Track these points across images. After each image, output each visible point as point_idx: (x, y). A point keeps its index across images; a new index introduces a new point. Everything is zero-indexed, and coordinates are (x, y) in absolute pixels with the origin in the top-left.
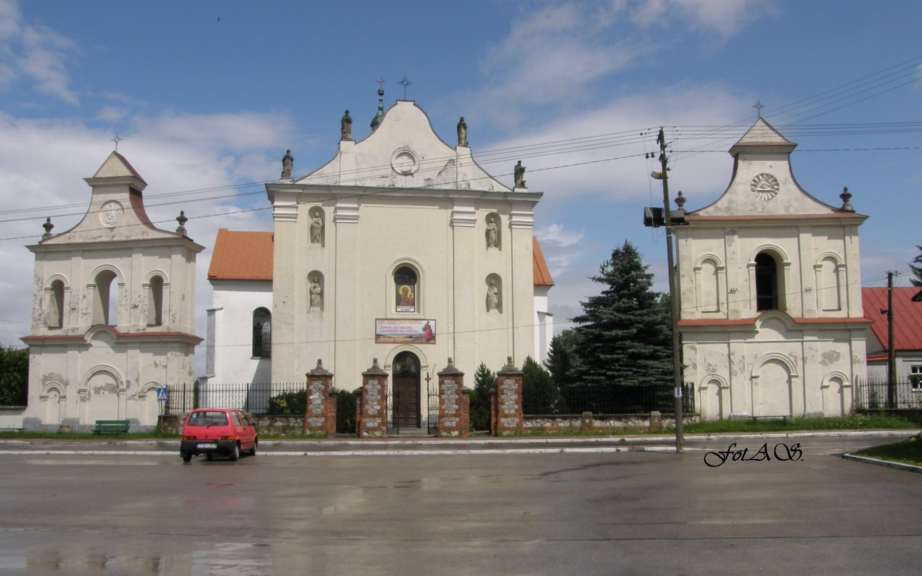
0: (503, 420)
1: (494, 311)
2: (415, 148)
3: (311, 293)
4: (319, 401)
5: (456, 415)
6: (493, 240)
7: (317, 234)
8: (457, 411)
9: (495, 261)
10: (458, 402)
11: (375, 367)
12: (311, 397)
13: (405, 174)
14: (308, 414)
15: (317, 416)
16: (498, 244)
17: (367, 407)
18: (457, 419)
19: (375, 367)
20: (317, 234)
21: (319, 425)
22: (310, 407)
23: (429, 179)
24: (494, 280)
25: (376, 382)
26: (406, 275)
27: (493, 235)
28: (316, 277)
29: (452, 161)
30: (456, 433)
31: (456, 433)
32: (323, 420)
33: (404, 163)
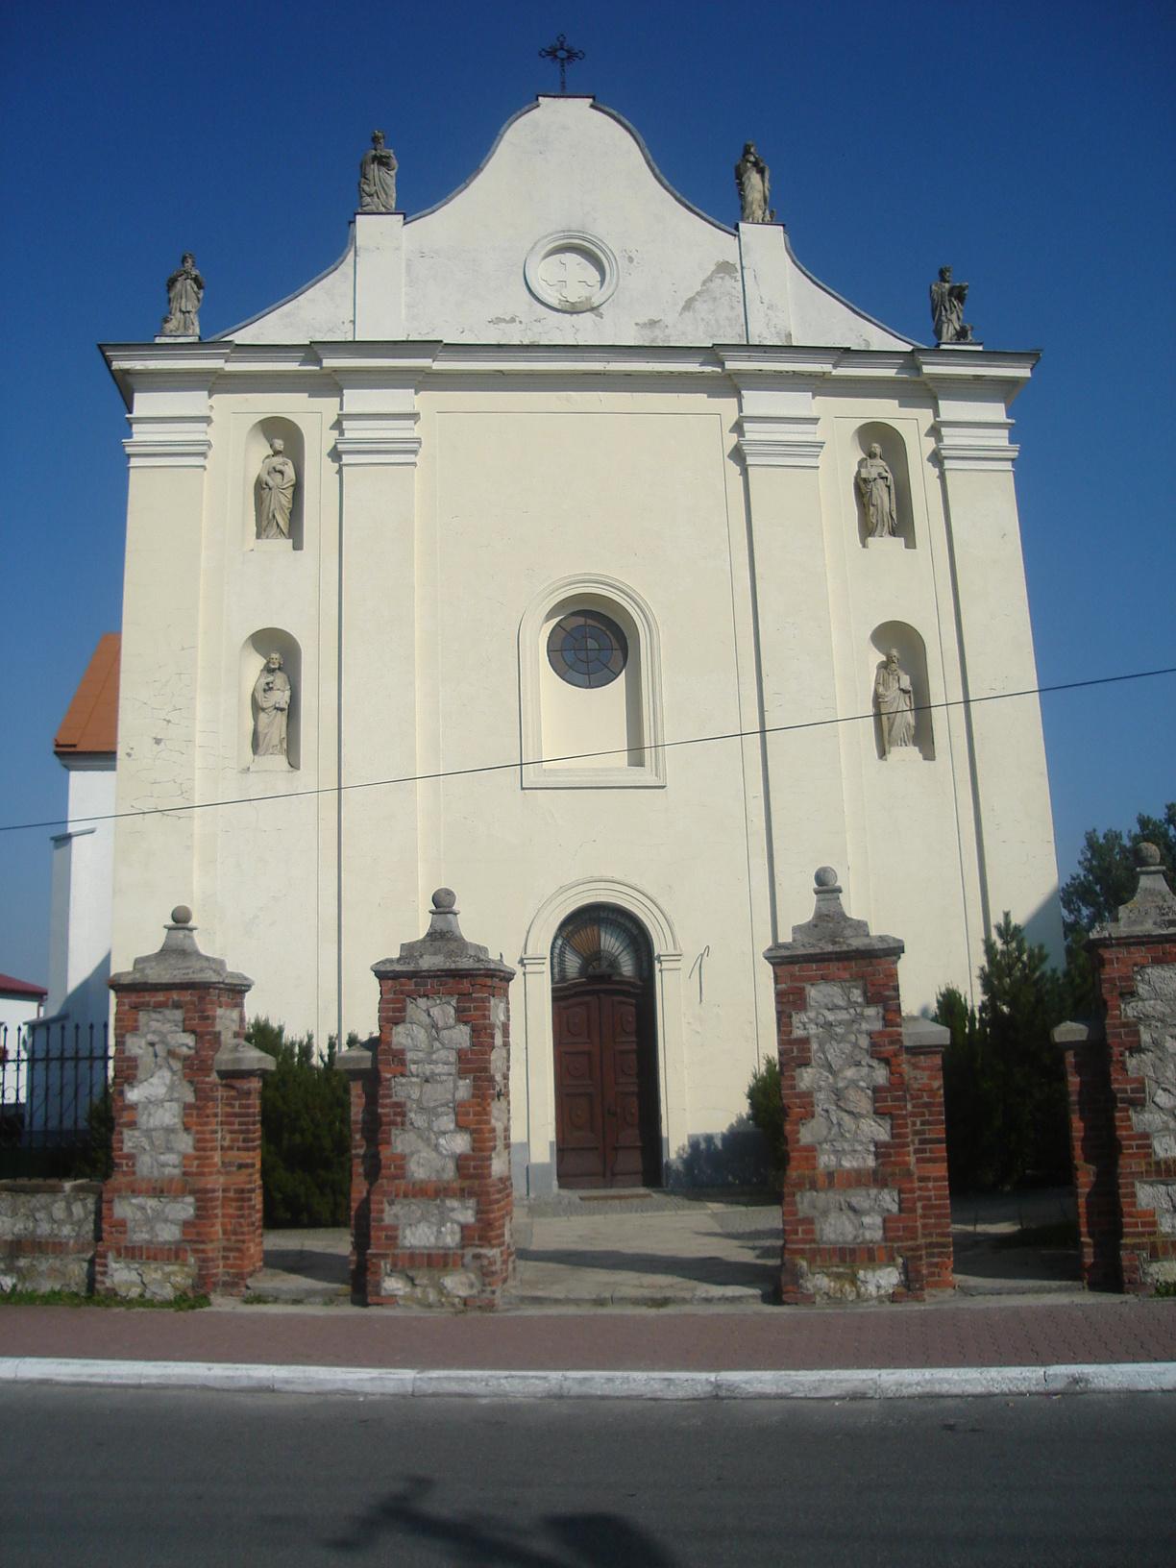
0: (1148, 1195)
1: (906, 754)
2: (606, 233)
3: (257, 708)
4: (168, 1116)
5: (878, 1179)
6: (884, 507)
7: (279, 510)
8: (881, 1151)
9: (900, 582)
10: (885, 1101)
11: (441, 936)
12: (133, 1095)
13: (573, 310)
14: (118, 1179)
15: (158, 1191)
16: (902, 526)
17: (401, 1142)
18: (889, 1200)
19: (441, 936)
20: (279, 510)
21: (169, 1233)
22: (129, 1141)
23: (653, 323)
24: (900, 645)
25: (443, 1011)
26: (594, 640)
27: (883, 497)
28: (278, 650)
29: (724, 268)
30: (888, 1278)
31: (888, 1278)
32: (184, 1208)
33: (573, 277)
